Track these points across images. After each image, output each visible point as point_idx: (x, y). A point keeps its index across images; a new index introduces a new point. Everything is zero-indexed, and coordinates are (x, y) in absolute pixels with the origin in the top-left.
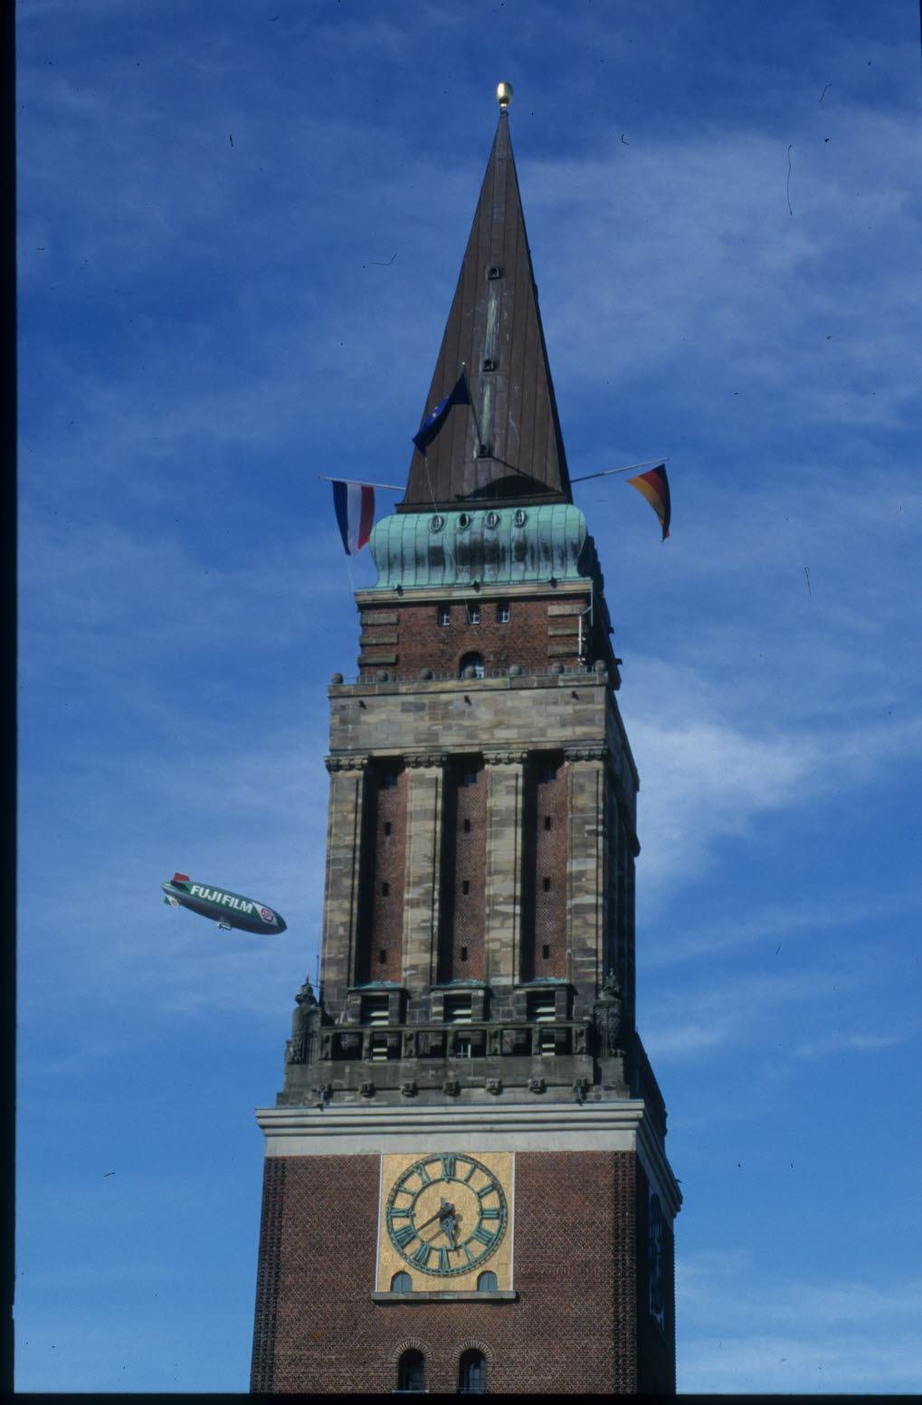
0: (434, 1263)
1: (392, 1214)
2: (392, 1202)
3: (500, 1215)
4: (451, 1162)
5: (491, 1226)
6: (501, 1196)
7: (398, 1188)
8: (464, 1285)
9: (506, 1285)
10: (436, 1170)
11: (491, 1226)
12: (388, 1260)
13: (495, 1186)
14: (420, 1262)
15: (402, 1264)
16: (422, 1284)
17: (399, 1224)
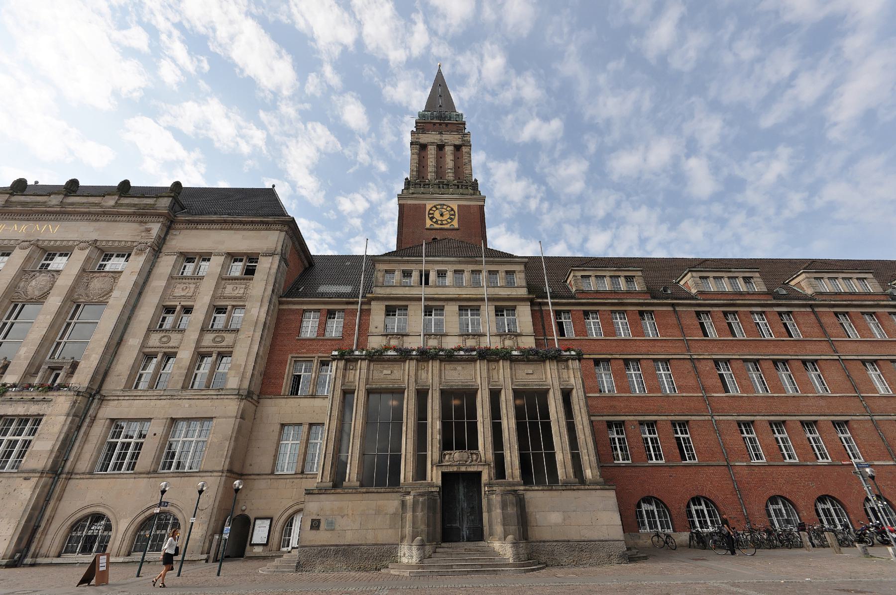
0: (439, 222)
1: (429, 214)
2: (429, 211)
3: (454, 215)
4: (441, 205)
5: (453, 217)
6: (454, 212)
7: (431, 210)
8: (448, 226)
9: (456, 226)
11: (453, 217)
12: (428, 223)
13: (452, 210)
14: (436, 222)
16: (436, 226)
17: (430, 216)
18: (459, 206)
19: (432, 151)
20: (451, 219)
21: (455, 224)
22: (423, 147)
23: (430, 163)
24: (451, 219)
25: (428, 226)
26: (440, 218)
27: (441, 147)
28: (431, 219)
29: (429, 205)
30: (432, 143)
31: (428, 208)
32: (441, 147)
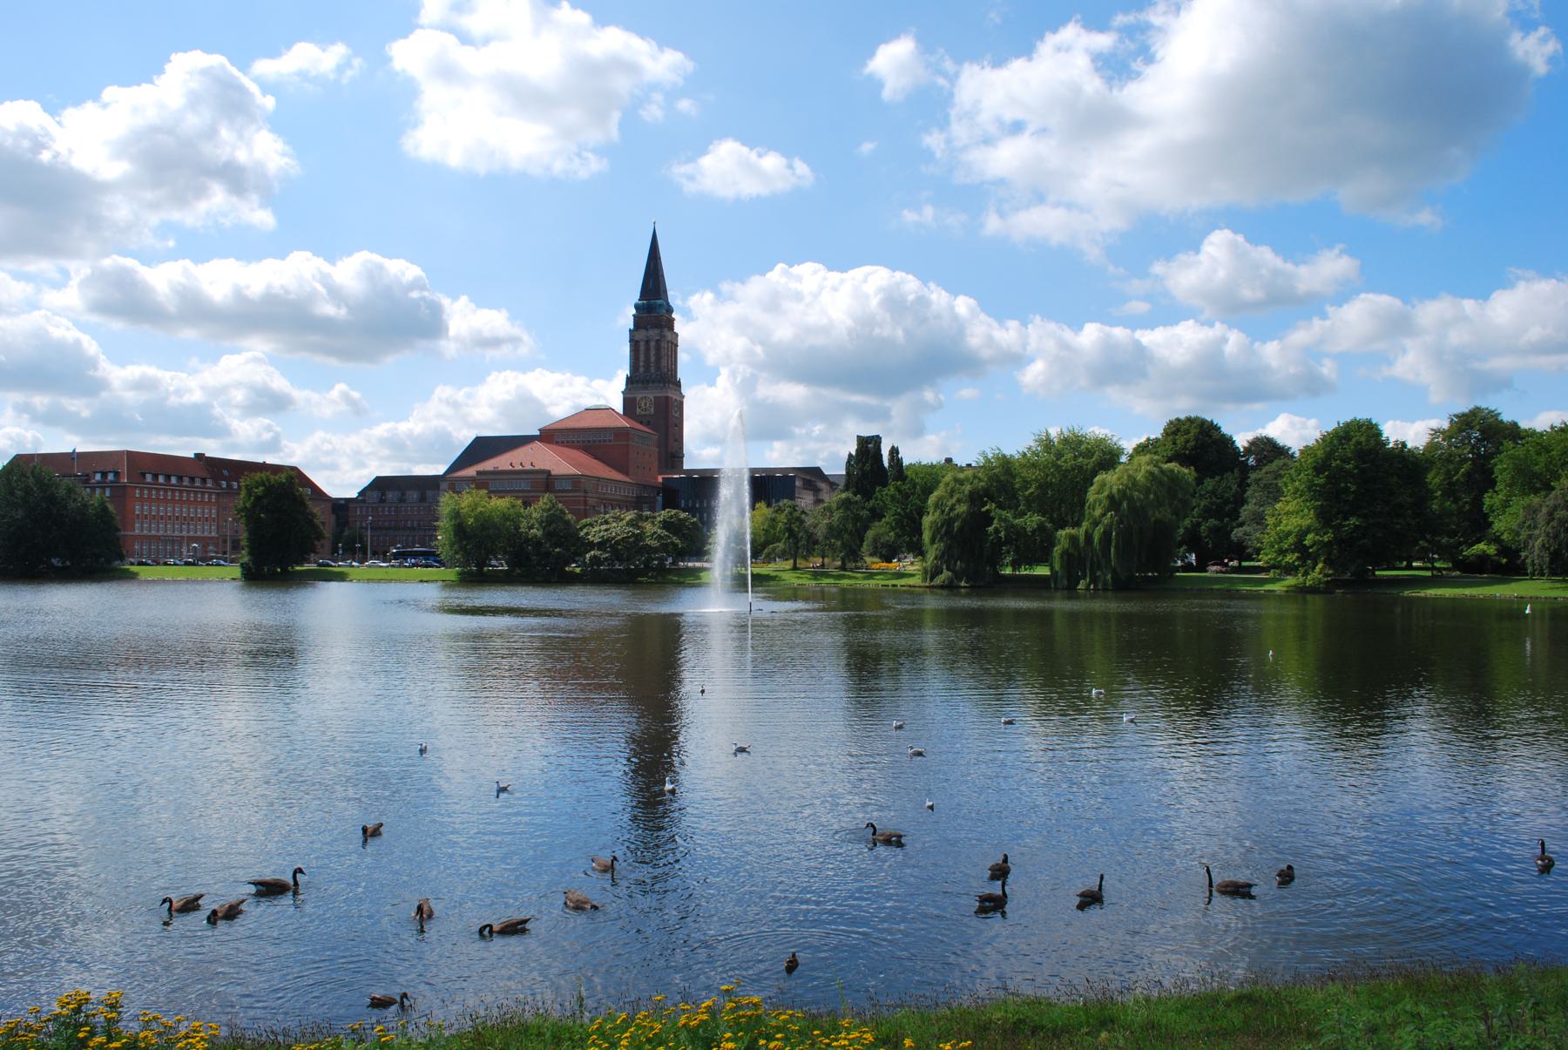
12: (638, 410)
19: (642, 347)
22: (637, 342)
27: (647, 342)
29: (639, 396)
32: (647, 342)
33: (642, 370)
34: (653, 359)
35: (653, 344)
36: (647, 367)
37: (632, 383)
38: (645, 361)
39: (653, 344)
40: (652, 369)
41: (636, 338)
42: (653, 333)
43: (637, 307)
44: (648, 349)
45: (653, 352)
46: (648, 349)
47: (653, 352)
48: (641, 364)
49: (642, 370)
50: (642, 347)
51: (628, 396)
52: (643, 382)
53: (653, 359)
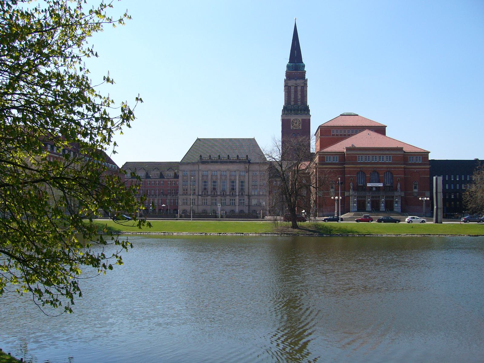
7: (292, 121)
9: (301, 128)
10: (295, 120)
12: (292, 127)
14: (294, 127)
15: (292, 127)
16: (295, 128)
18: (302, 119)
19: (293, 90)
20: (299, 125)
21: (301, 127)
23: (292, 97)
24: (299, 125)
25: (291, 128)
26: (295, 125)
27: (296, 87)
28: (293, 125)
30: (293, 86)
31: (291, 121)
32: (296, 87)
33: (292, 103)
34: (299, 97)
35: (299, 88)
36: (296, 101)
37: (288, 111)
38: (294, 98)
39: (299, 88)
40: (299, 103)
41: (289, 85)
42: (299, 82)
43: (288, 67)
44: (296, 92)
45: (299, 93)
46: (296, 92)
47: (299, 93)
48: (292, 100)
49: (292, 103)
50: (293, 88)
51: (285, 118)
52: (294, 110)
53: (299, 97)
